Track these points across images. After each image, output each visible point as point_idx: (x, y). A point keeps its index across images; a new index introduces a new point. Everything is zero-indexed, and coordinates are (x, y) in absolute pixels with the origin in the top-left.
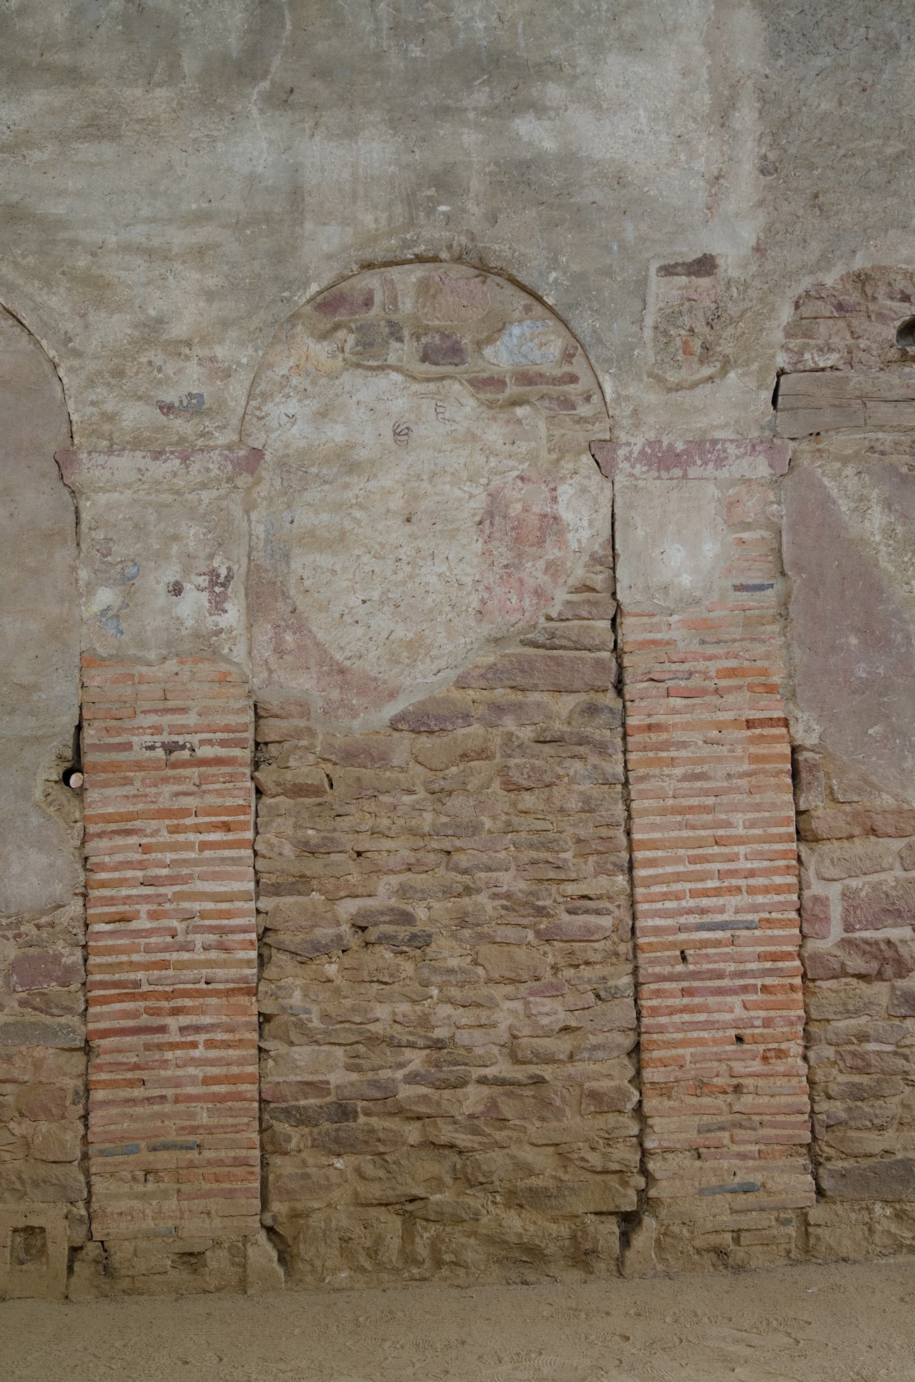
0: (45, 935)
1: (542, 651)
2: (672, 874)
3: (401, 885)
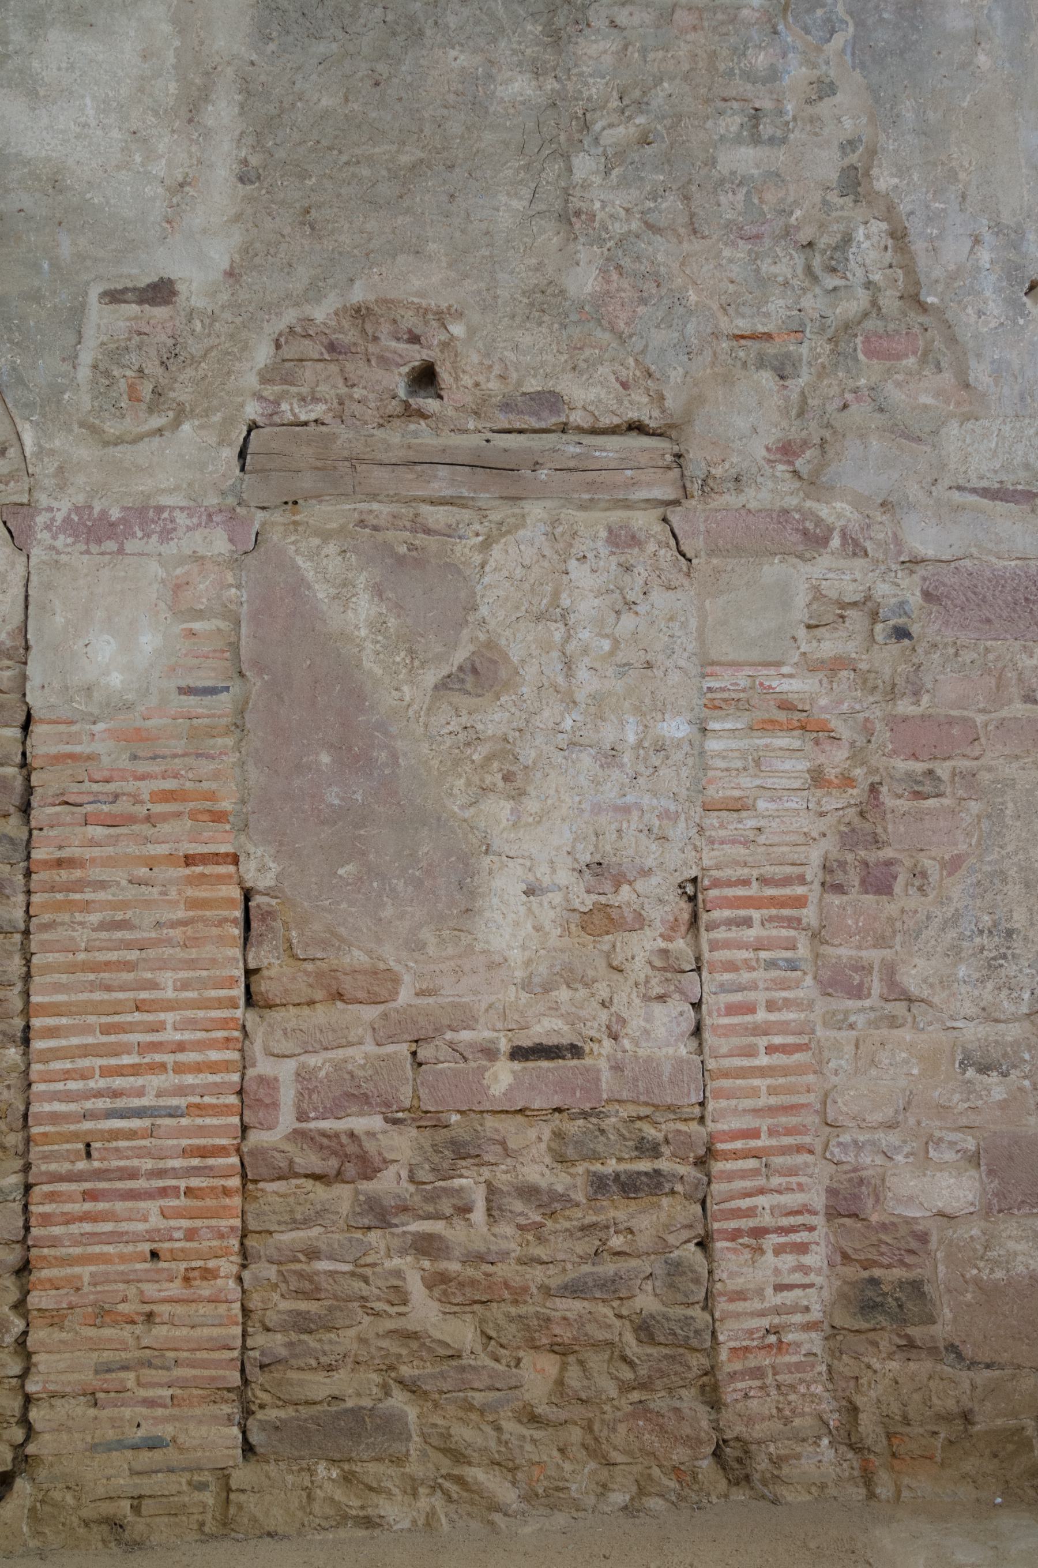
2: (78, 1047)
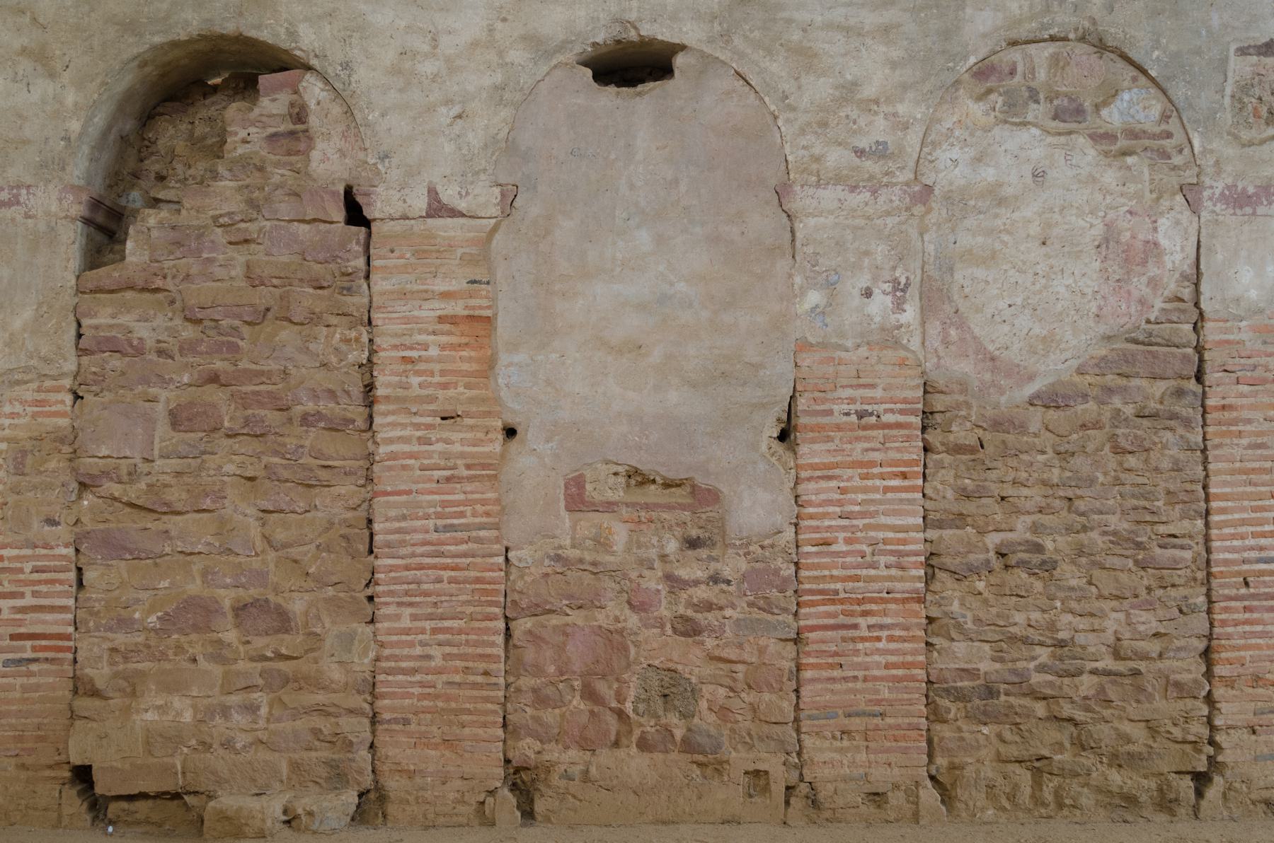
0: (767, 554)
1: (1141, 347)
3: (1034, 523)
